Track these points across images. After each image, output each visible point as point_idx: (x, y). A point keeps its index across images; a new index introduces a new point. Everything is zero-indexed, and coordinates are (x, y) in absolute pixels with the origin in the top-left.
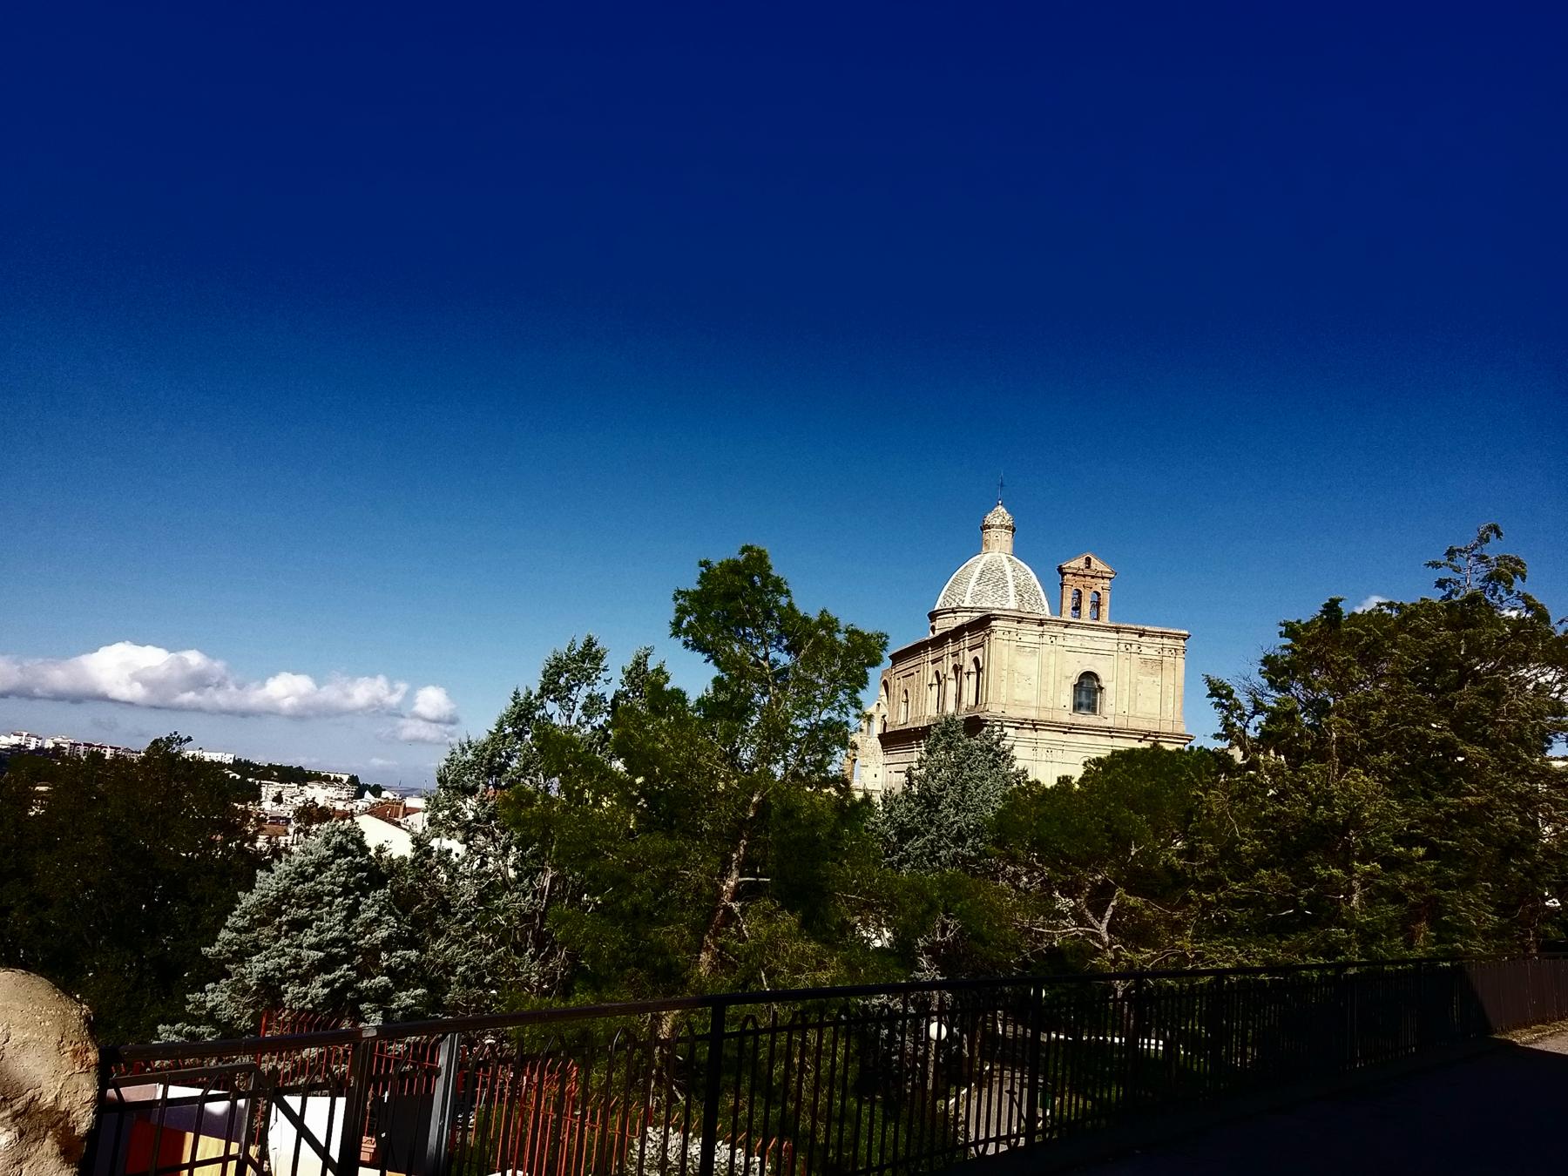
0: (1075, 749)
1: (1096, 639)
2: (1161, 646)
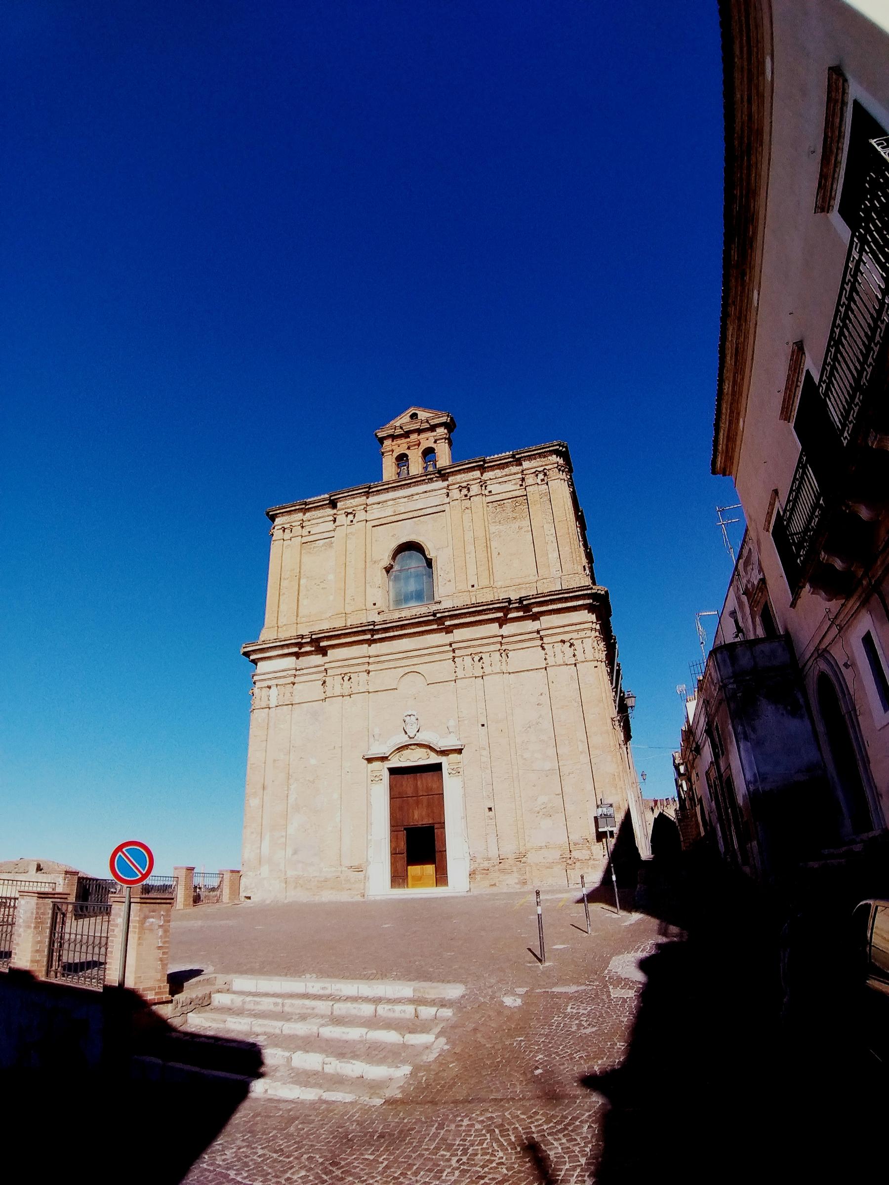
0: (392, 664)
1: (416, 497)
2: (520, 476)
